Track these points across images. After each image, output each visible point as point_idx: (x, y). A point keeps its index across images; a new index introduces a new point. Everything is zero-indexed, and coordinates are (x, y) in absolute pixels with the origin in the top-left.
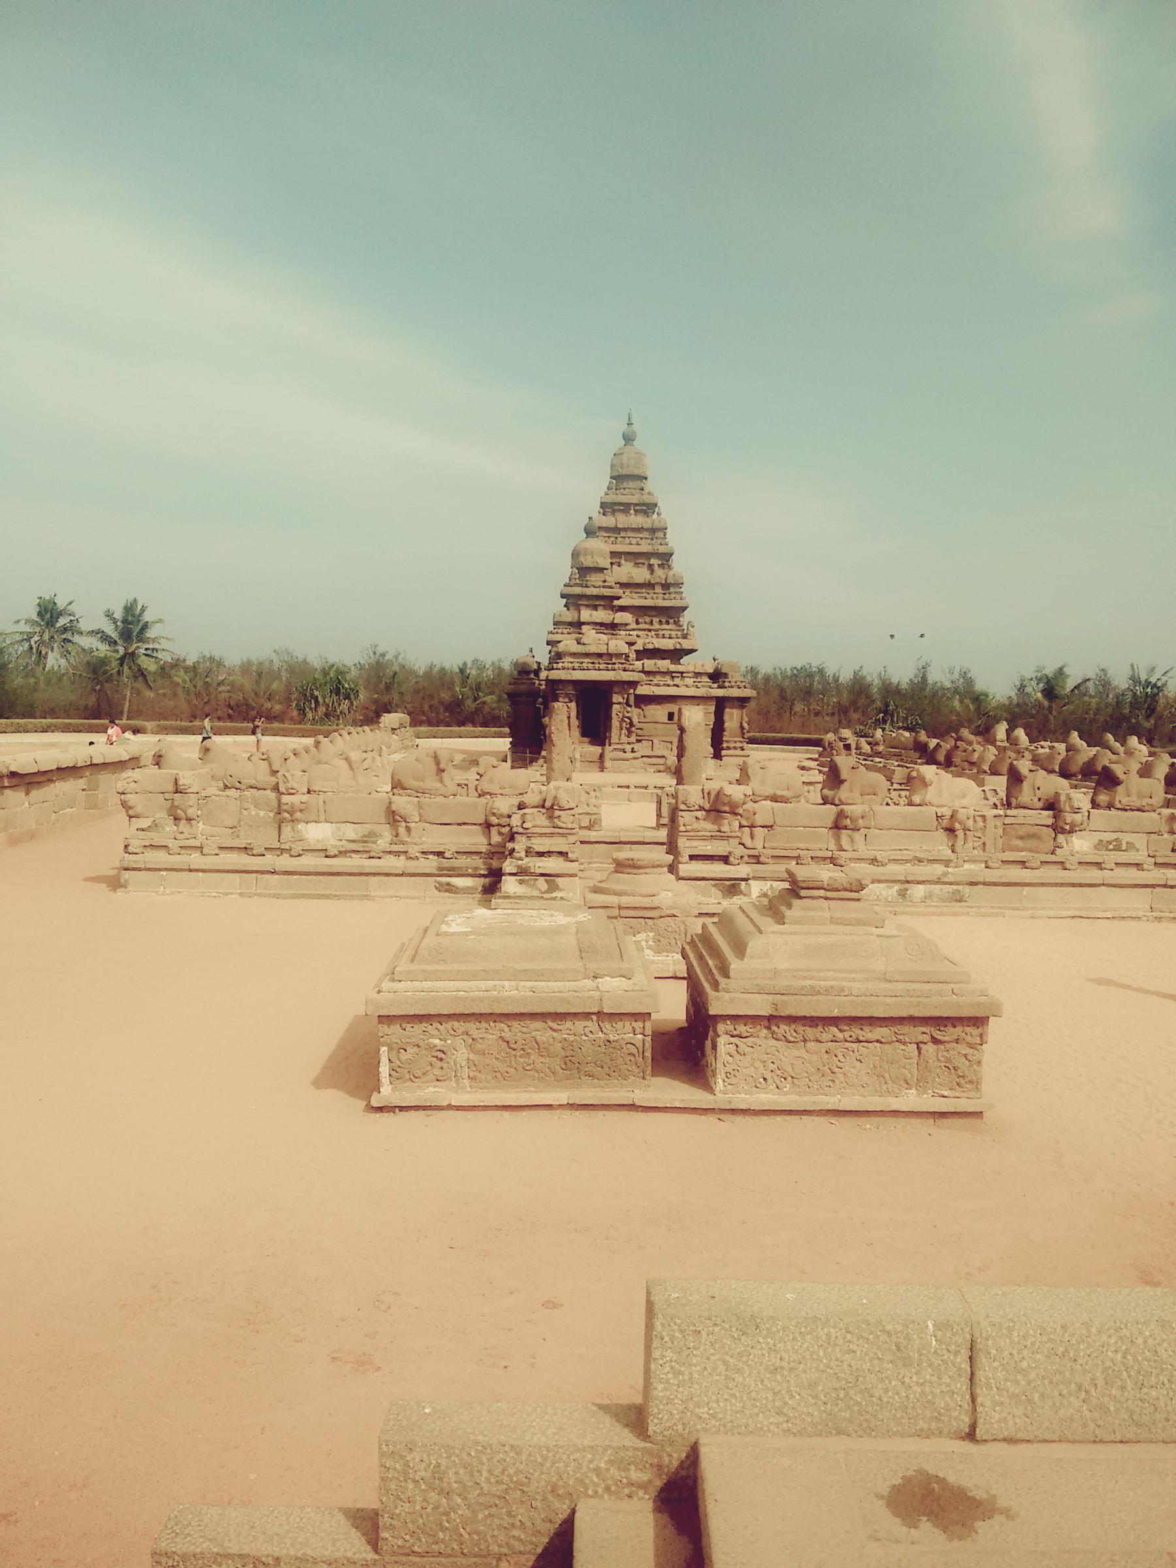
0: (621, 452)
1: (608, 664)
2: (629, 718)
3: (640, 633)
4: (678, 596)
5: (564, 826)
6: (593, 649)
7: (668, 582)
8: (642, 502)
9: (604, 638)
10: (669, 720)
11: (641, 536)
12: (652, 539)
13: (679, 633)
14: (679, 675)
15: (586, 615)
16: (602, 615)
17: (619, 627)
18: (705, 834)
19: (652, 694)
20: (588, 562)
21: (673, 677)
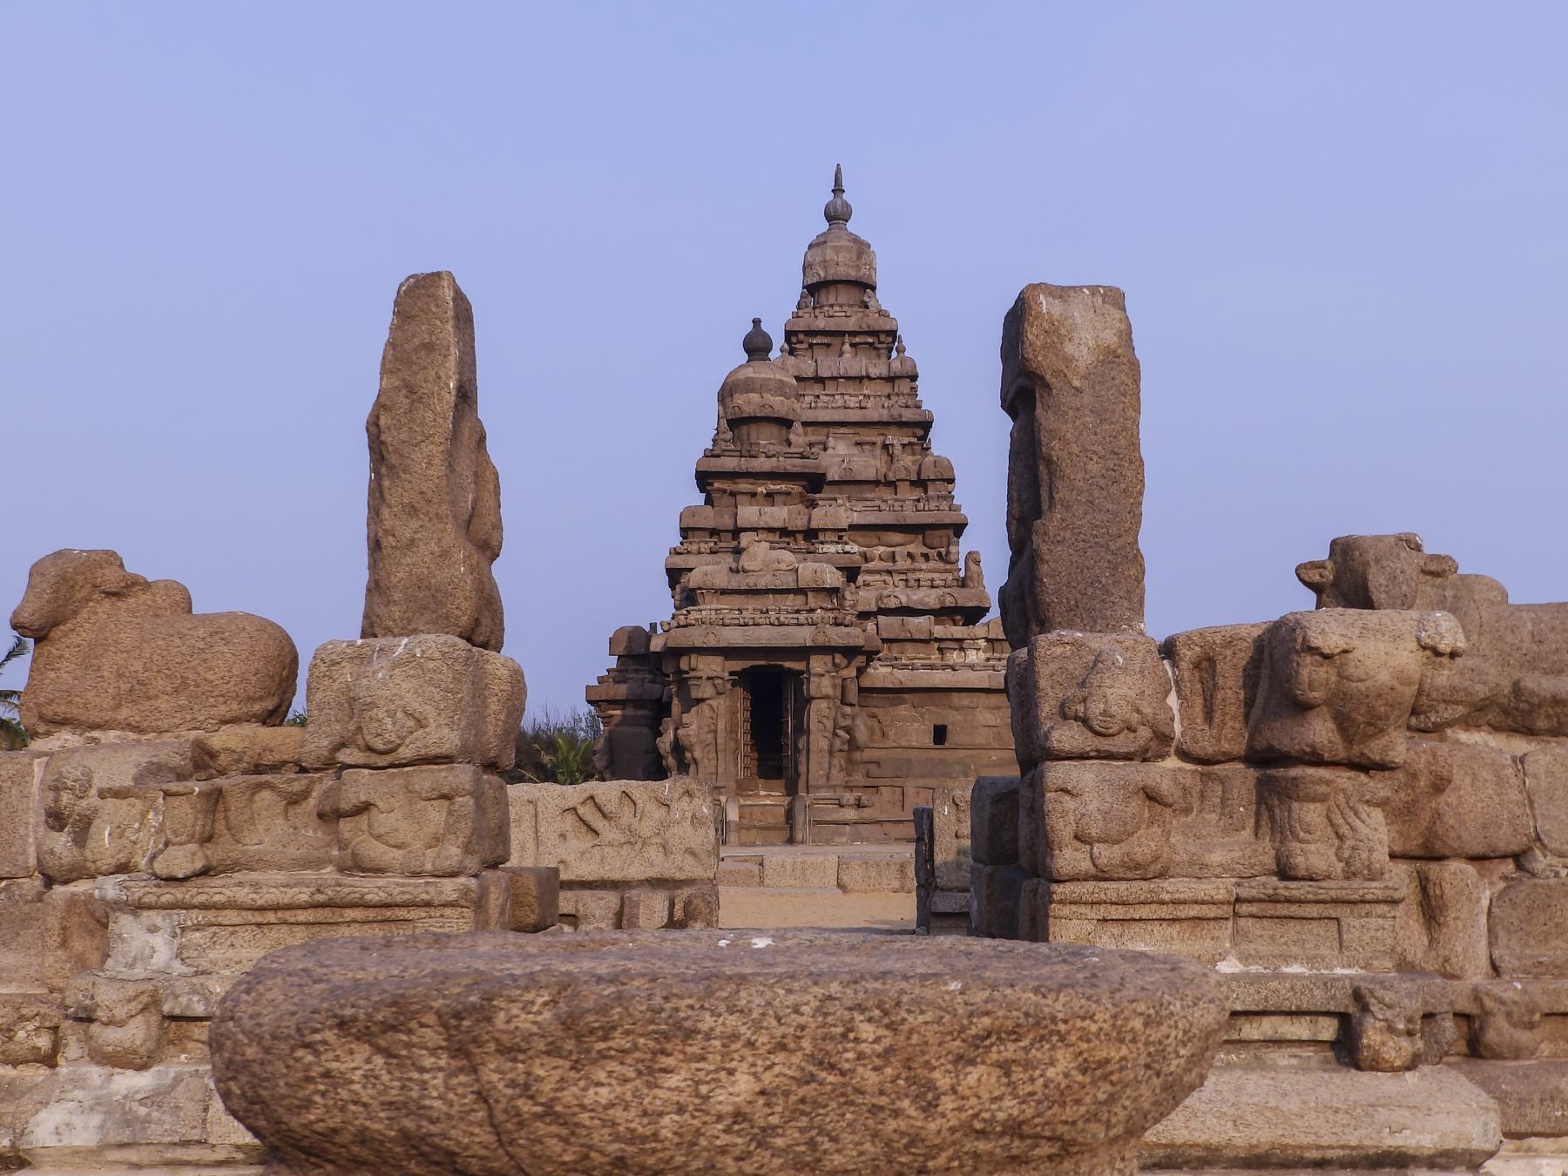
0: (822, 239)
1: (798, 612)
2: (848, 730)
4: (944, 505)
5: (394, 856)
6: (763, 582)
9: (787, 556)
11: (866, 392)
13: (950, 577)
15: (749, 513)
16: (779, 514)
17: (821, 538)
18: (1206, 889)
19: (899, 686)
20: (748, 403)
21: (940, 650)
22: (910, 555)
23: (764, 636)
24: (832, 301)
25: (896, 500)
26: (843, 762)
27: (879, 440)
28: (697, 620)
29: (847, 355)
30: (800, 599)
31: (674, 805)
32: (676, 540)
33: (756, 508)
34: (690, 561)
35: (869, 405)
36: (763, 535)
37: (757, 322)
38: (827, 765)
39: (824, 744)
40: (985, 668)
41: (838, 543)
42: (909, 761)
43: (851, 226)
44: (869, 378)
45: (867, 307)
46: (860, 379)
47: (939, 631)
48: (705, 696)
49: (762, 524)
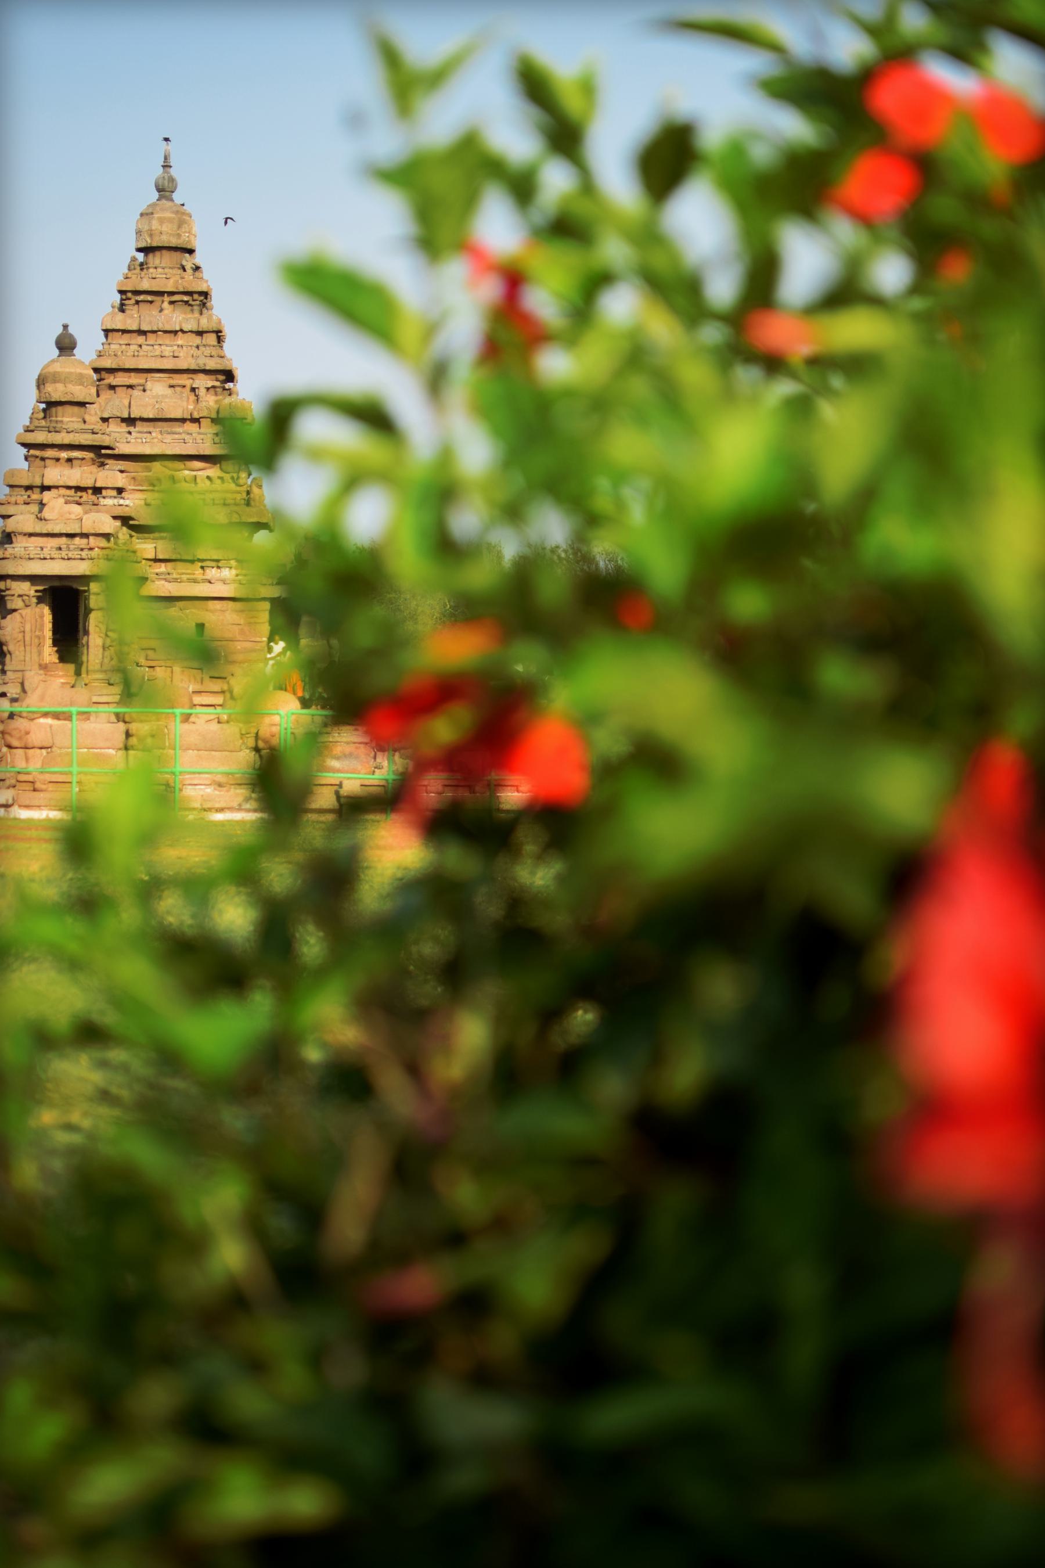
0: (150, 210)
1: (82, 550)
8: (181, 290)
9: (77, 509)
11: (180, 342)
15: (54, 474)
17: (104, 492)
20: (56, 391)
21: (202, 568)
22: (208, 478)
25: (199, 433)
28: (11, 554)
30: (84, 541)
35: (181, 354)
36: (63, 491)
37: (65, 327)
38: (101, 656)
44: (182, 331)
45: (185, 270)
46: (175, 332)
48: (17, 608)
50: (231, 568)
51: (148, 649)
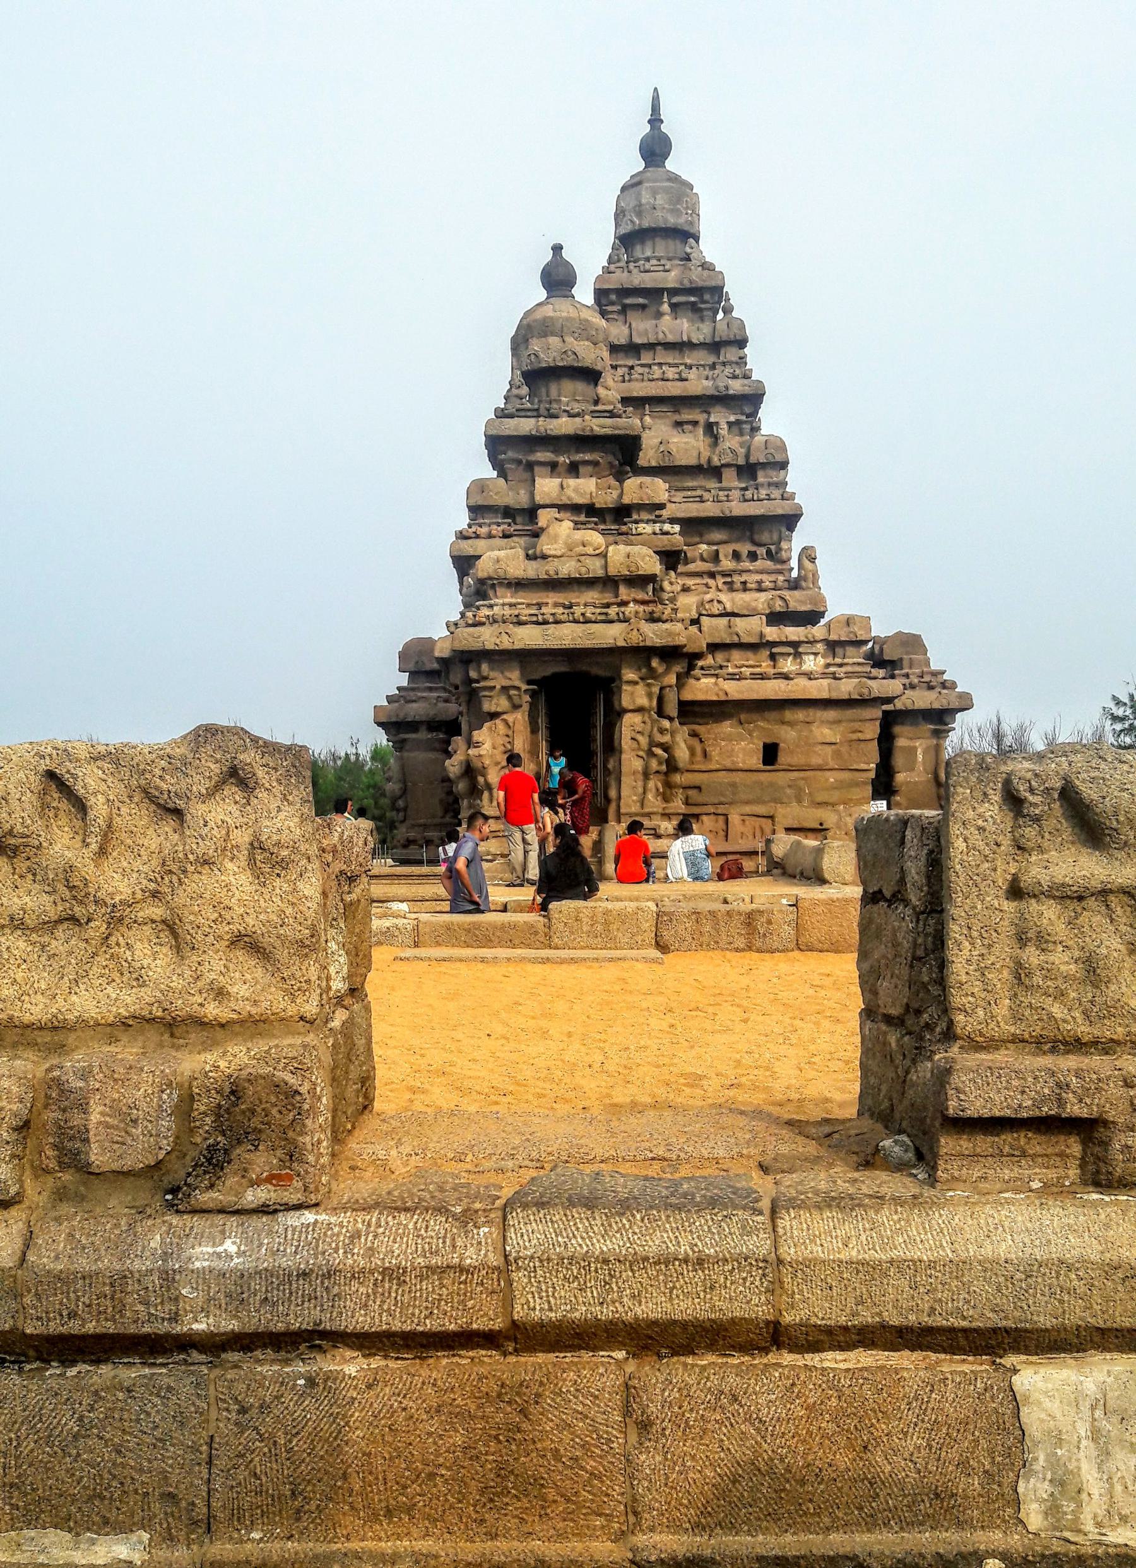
1: (608, 606)
2: (666, 748)
3: (690, 582)
4: (776, 493)
6: (567, 568)
7: (752, 460)
8: (687, 284)
9: (595, 538)
10: (765, 763)
11: (688, 361)
12: (713, 367)
13: (781, 578)
14: (791, 650)
15: (547, 487)
17: (635, 517)
19: (723, 698)
21: (773, 657)
23: (567, 636)
24: (648, 253)
25: (721, 489)
26: (660, 785)
27: (701, 418)
29: (667, 317)
31: (197, 810)
32: (462, 520)
33: (557, 481)
34: (480, 545)
37: (557, 249)
38: (640, 790)
39: (638, 765)
40: (824, 675)
41: (655, 522)
42: (733, 785)
43: (671, 165)
47: (772, 633)
49: (565, 500)
50: (816, 654)
51: (690, 787)
